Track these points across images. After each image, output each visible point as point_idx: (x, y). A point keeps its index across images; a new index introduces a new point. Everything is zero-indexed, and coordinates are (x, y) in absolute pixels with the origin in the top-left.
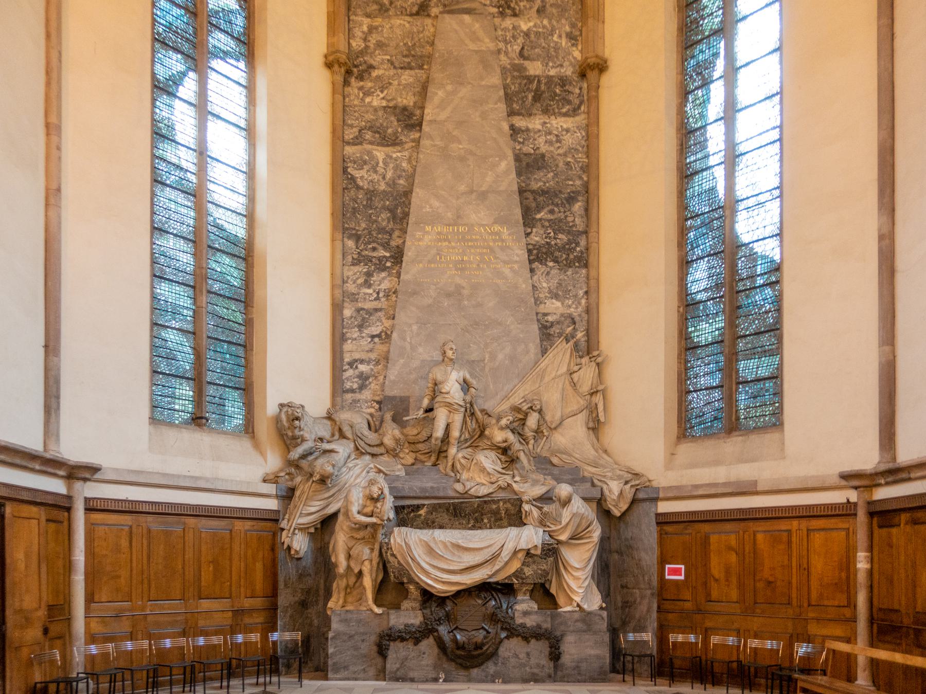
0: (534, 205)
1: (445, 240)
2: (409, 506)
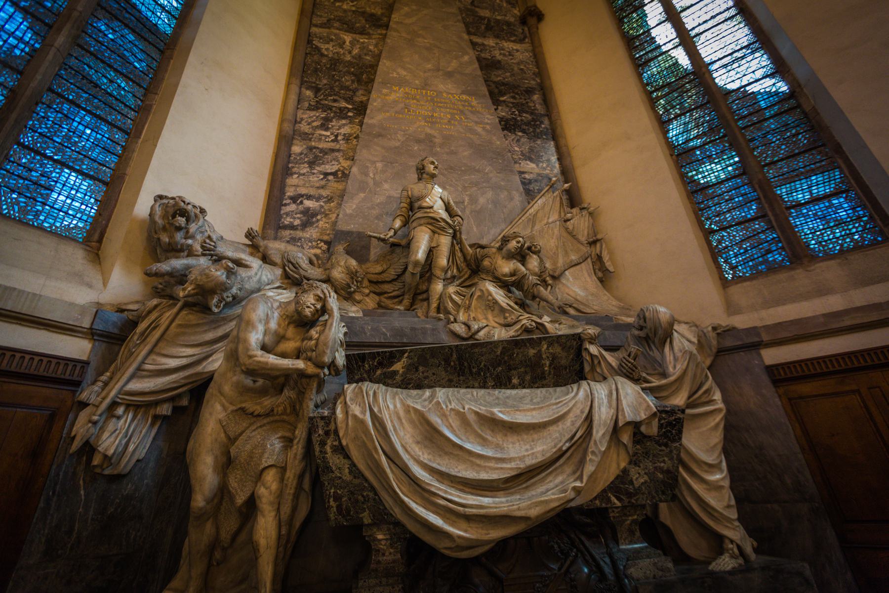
0: (496, 91)
1: (413, 99)
2: (373, 356)
